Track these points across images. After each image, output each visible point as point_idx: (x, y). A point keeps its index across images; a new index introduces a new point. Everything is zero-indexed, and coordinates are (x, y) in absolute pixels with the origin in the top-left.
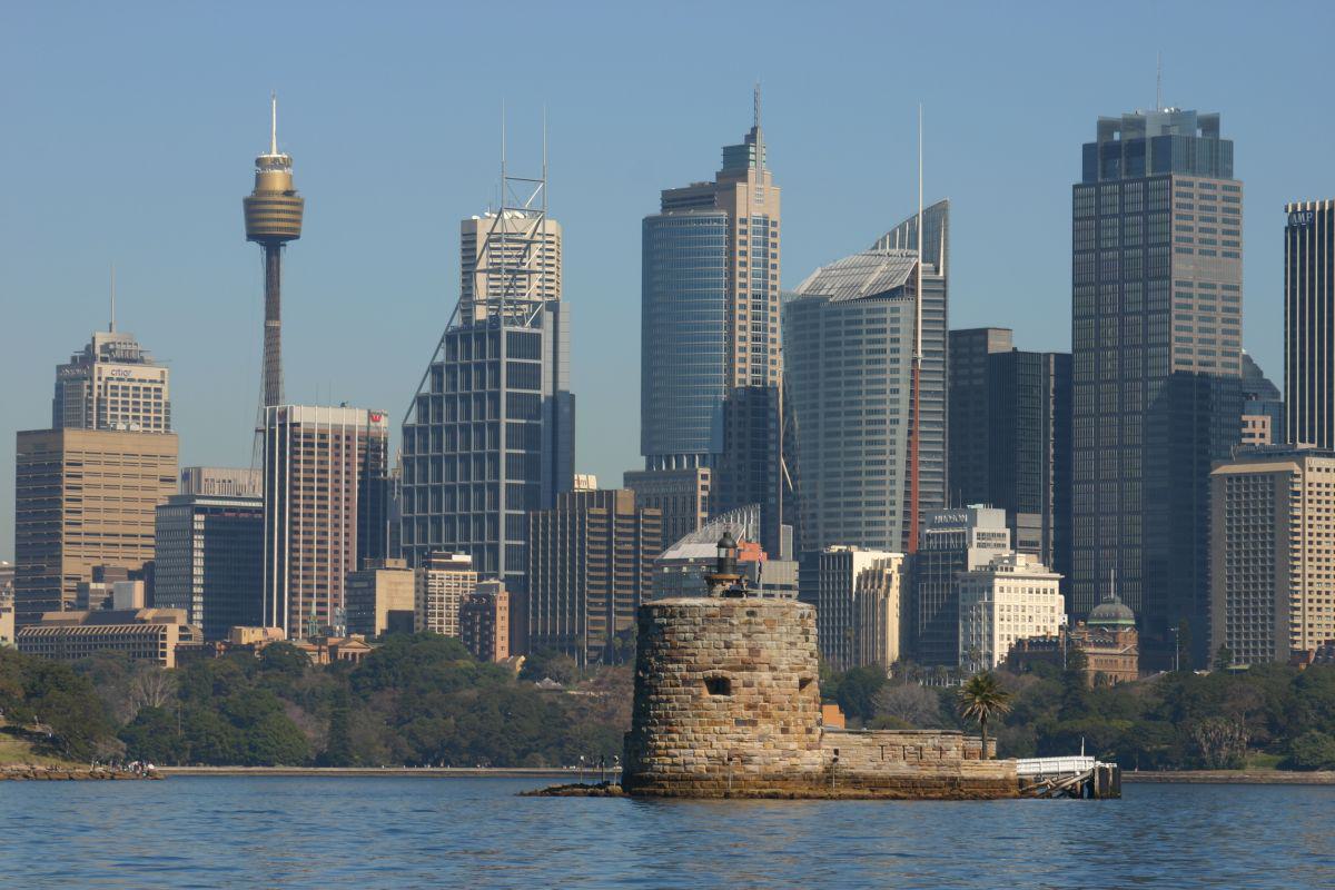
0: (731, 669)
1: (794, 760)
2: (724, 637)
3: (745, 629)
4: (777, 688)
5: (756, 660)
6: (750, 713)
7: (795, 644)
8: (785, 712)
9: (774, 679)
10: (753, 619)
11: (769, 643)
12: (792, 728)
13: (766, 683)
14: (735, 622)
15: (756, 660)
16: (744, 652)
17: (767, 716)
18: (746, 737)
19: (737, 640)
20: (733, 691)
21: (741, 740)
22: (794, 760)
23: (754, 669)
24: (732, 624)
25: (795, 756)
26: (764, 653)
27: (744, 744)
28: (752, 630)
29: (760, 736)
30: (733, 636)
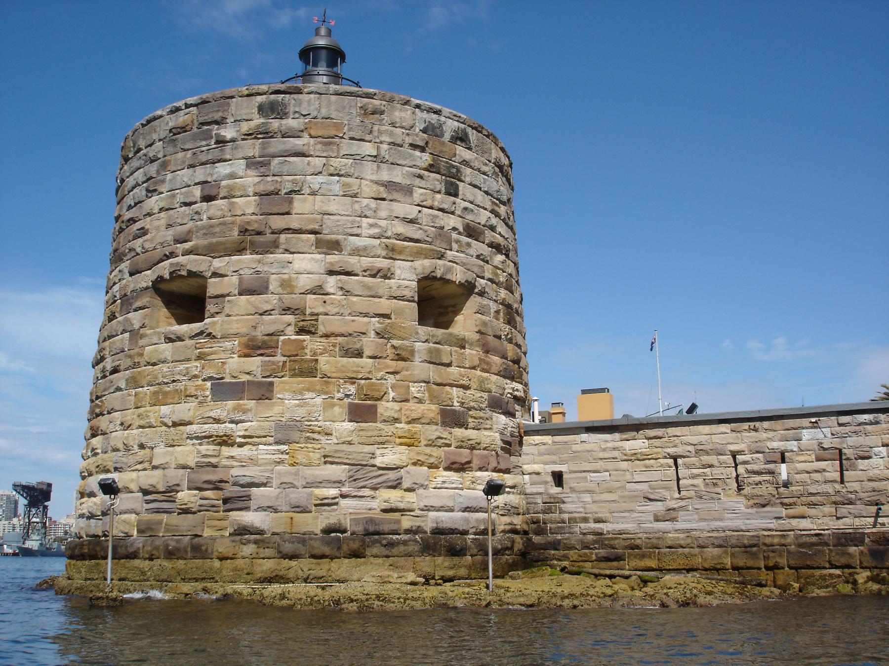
0: (212, 251)
1: (394, 497)
2: (200, 174)
3: (252, 148)
4: (339, 297)
5: (278, 222)
6: (255, 363)
7: (408, 191)
8: (365, 361)
9: (331, 273)
10: (275, 124)
11: (315, 182)
12: (386, 408)
13: (305, 282)
14: (228, 133)
15: (278, 222)
16: (247, 205)
17: (308, 370)
18: (239, 430)
19: (232, 176)
20: (210, 307)
21: (225, 441)
22: (394, 497)
23: (272, 247)
24: (221, 141)
25: (396, 485)
26: (302, 205)
27: (235, 451)
28: (272, 150)
29: (280, 426)
30: (223, 169)
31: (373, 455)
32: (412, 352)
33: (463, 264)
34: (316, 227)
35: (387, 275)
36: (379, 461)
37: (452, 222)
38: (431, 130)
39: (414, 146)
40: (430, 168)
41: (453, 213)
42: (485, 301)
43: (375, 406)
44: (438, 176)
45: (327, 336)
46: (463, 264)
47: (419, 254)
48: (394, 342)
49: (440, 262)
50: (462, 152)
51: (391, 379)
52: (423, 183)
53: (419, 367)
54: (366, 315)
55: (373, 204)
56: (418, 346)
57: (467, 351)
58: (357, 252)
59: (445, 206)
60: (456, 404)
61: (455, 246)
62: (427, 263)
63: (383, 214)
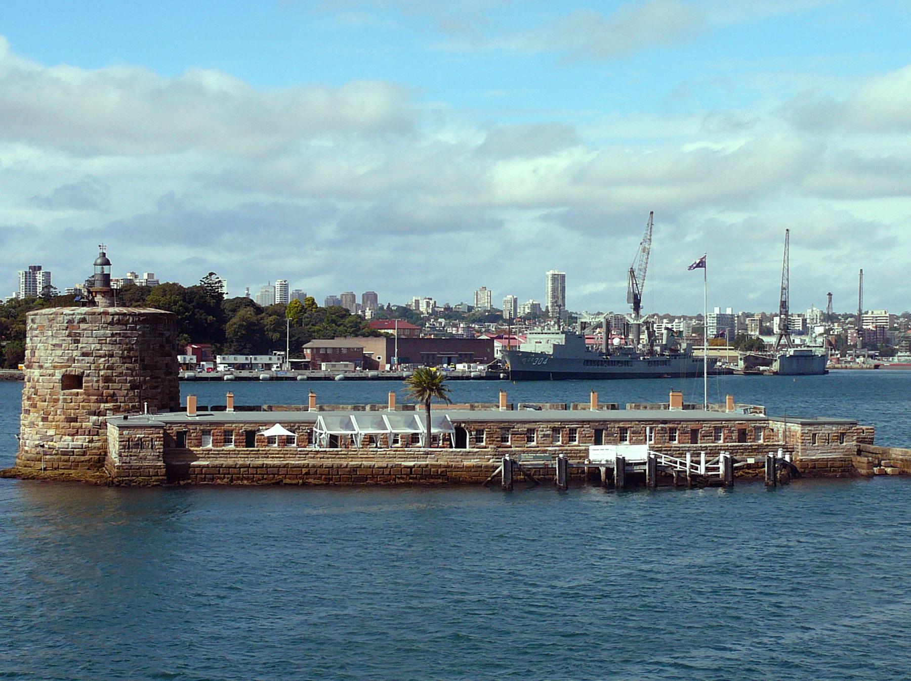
9: (41, 376)
12: (50, 417)
25: (52, 441)
28: (34, 334)
31: (46, 432)
32: (58, 400)
33: (79, 368)
34: (38, 361)
35: (53, 375)
36: (48, 434)
37: (75, 353)
38: (69, 322)
39: (63, 330)
40: (68, 336)
41: (77, 350)
42: (89, 378)
43: (48, 417)
44: (71, 338)
45: (39, 396)
46: (79, 368)
47: (62, 367)
48: (54, 397)
49: (68, 369)
50: (82, 326)
51: (52, 409)
52: (65, 342)
53: (60, 403)
54: (47, 389)
55: (50, 352)
56: (61, 397)
57: (79, 397)
58: (47, 368)
59: (73, 349)
60: (72, 415)
61: (76, 362)
62: (64, 370)
63: (53, 355)
